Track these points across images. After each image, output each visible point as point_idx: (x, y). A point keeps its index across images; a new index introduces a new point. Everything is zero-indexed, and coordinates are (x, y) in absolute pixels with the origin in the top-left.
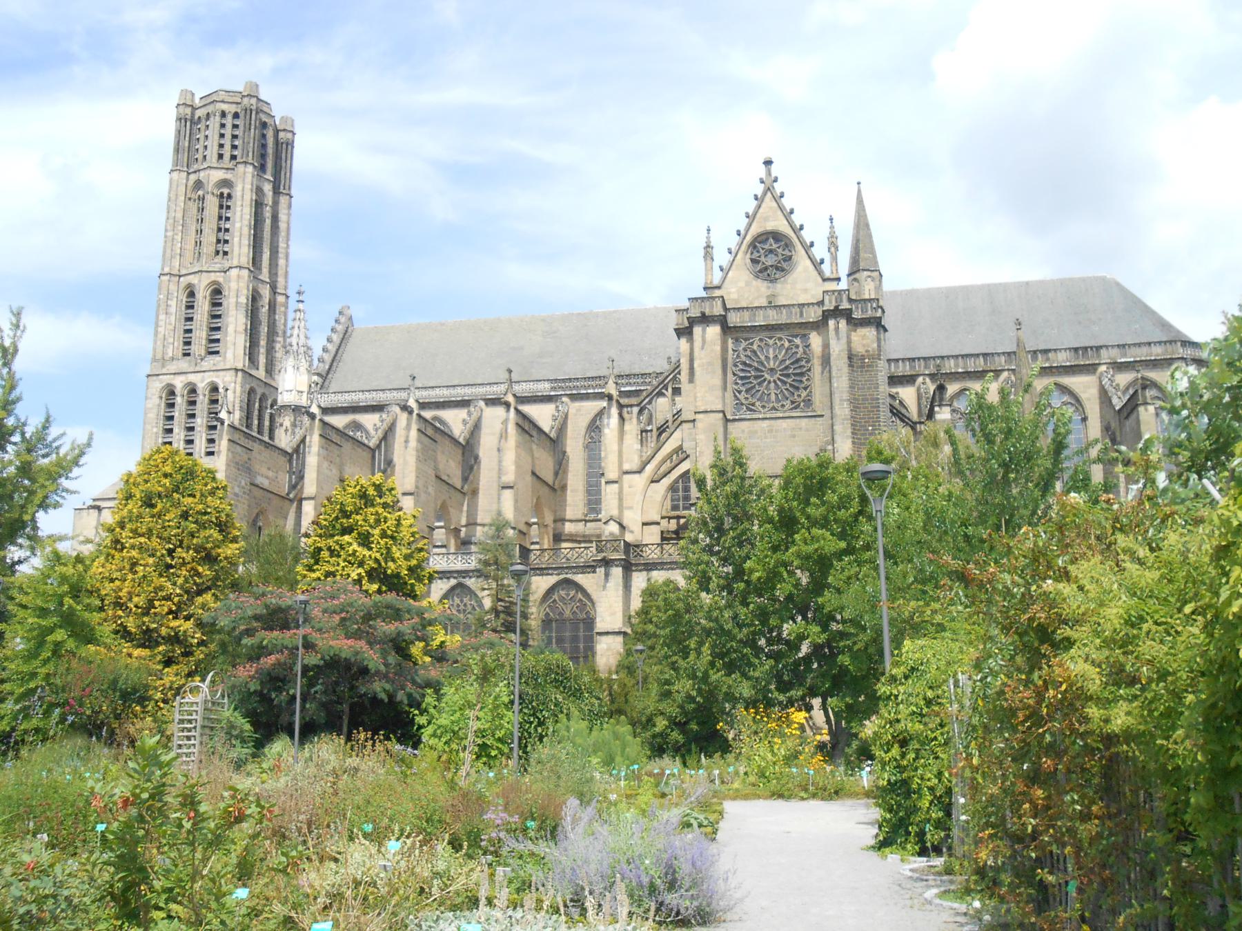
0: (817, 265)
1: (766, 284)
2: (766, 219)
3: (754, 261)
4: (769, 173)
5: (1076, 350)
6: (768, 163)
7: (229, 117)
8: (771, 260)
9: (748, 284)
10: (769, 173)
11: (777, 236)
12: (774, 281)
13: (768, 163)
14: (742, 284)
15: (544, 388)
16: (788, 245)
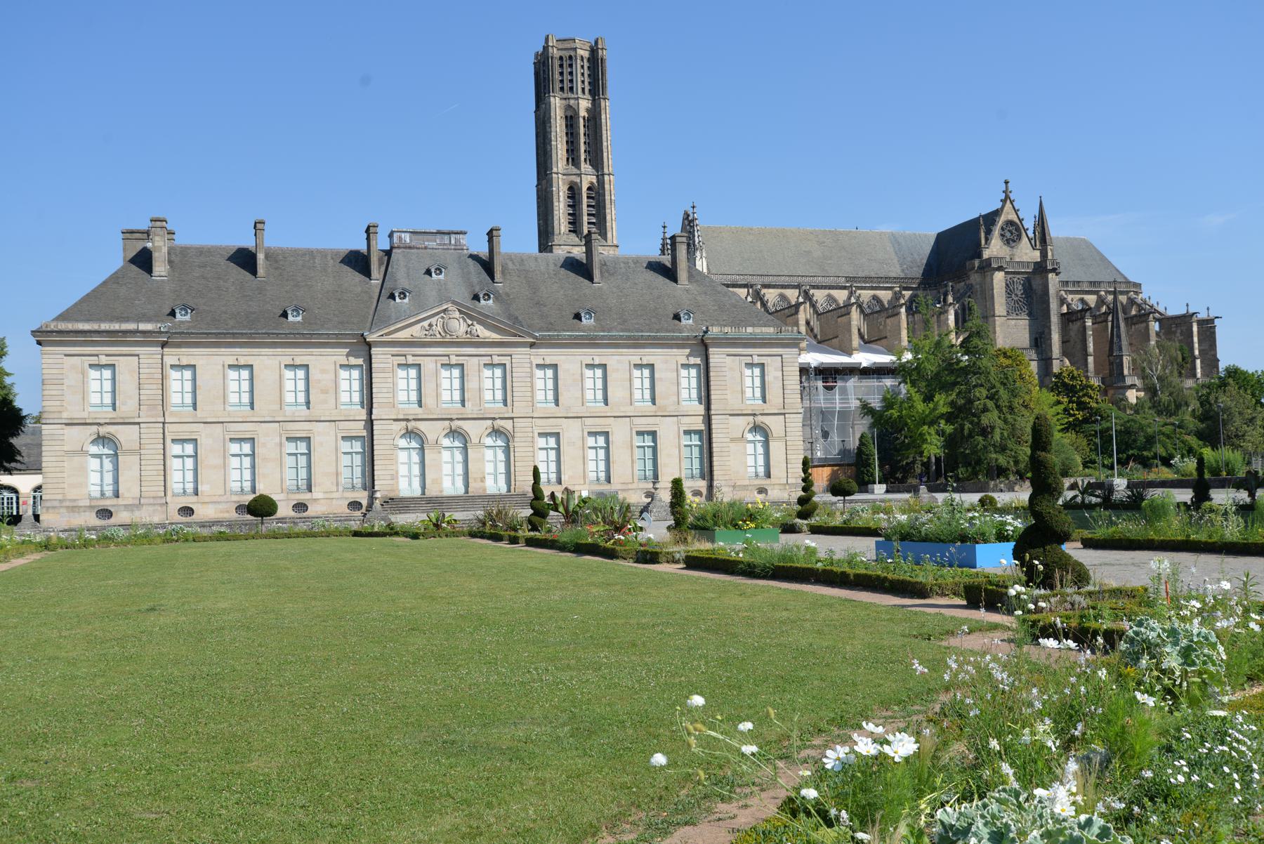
0: (1030, 240)
1: (1009, 248)
2: (1008, 213)
3: (1002, 235)
4: (1007, 187)
5: (1091, 282)
6: (1006, 182)
7: (585, 61)
8: (1008, 235)
9: (1001, 247)
10: (1007, 187)
11: (1011, 223)
12: (1012, 247)
13: (1006, 182)
14: (998, 247)
15: (842, 281)
16: (1018, 229)
